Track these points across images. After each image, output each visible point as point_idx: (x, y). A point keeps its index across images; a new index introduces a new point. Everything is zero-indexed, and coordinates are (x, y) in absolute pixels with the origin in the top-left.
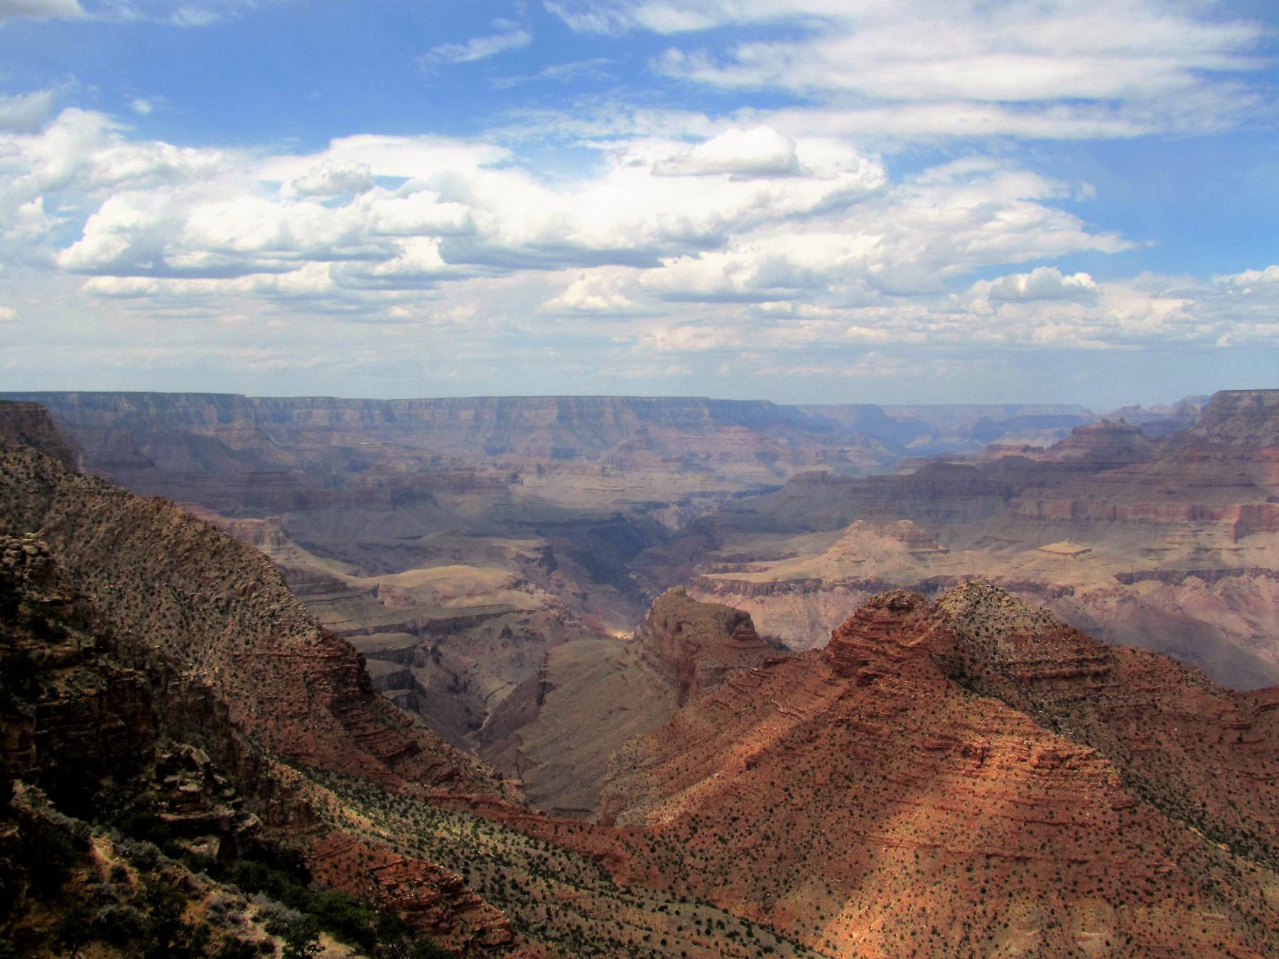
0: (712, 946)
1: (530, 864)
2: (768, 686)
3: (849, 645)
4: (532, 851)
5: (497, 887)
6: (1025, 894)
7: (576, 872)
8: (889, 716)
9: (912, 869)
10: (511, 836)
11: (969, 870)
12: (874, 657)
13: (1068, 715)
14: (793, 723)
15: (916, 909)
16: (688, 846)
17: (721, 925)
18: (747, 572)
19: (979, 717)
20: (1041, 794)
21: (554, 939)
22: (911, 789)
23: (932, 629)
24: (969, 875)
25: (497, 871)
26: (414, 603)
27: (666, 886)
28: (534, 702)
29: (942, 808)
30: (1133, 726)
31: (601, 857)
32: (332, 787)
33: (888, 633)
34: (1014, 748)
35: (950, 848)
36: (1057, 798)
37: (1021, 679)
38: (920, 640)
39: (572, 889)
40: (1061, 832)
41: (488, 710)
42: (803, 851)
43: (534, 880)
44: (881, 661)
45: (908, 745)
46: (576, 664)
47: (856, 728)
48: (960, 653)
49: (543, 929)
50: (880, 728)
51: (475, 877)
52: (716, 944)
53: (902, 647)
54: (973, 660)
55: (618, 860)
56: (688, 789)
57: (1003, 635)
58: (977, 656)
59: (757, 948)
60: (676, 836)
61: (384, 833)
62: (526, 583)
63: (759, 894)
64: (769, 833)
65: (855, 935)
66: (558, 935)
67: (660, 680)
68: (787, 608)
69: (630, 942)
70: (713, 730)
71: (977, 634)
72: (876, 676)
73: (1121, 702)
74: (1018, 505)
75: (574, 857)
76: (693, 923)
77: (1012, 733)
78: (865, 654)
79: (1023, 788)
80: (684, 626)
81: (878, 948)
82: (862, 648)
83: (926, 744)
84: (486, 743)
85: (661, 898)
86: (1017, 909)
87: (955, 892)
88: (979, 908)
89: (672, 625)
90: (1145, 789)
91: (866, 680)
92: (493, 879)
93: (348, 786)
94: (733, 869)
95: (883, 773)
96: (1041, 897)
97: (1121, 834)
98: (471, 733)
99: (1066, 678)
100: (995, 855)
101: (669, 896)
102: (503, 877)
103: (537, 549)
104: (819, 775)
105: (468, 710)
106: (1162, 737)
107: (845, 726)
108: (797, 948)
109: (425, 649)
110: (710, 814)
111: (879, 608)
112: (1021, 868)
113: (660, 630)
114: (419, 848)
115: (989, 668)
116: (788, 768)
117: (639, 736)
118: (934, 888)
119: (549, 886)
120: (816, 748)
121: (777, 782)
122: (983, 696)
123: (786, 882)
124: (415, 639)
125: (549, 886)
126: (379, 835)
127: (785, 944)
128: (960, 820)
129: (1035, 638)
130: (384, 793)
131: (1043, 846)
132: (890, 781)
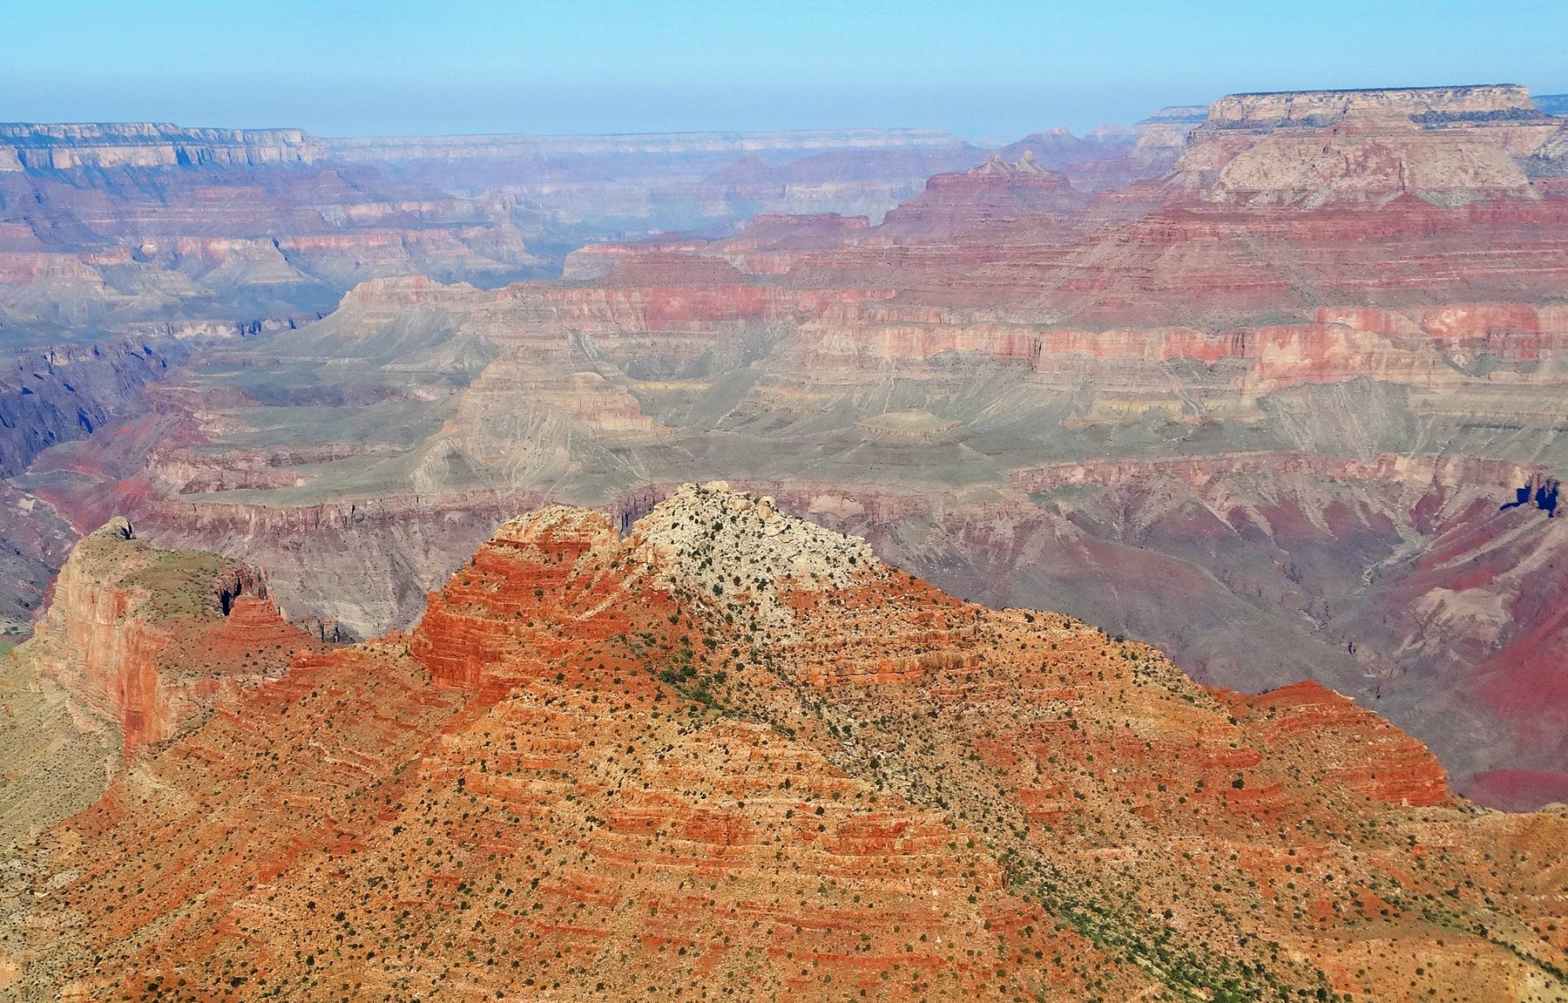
2: (302, 713)
13: (901, 747)
14: (356, 785)
20: (847, 906)
23: (626, 584)
30: (1033, 765)
38: (601, 608)
48: (683, 629)
57: (769, 592)
58: (718, 637)
70: (192, 806)
71: (718, 591)
73: (1006, 719)
78: (492, 641)
90: (1053, 888)
91: (499, 689)
97: (1001, 974)
104: (405, 887)
106: (1088, 785)
120: (397, 830)
122: (728, 715)
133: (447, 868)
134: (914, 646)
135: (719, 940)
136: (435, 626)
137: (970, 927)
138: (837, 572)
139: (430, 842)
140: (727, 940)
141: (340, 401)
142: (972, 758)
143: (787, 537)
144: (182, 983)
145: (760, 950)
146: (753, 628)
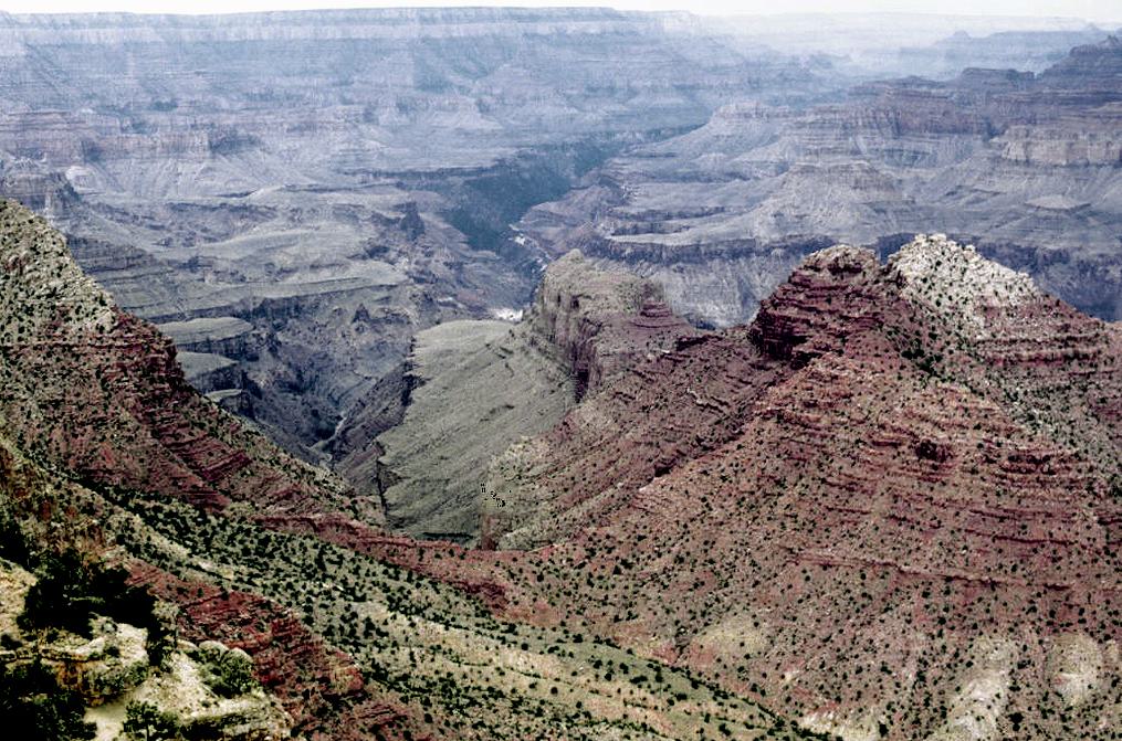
0: (614, 695)
1: (389, 598)
2: (683, 373)
3: (783, 317)
4: (390, 582)
5: (347, 628)
6: (993, 626)
7: (446, 607)
8: (830, 405)
9: (857, 592)
10: (365, 565)
11: (925, 595)
12: (812, 332)
14: (714, 418)
15: (863, 642)
16: (584, 571)
17: (624, 668)
18: (662, 232)
19: (939, 407)
21: (420, 689)
22: (856, 494)
24: (926, 602)
25: (347, 609)
26: (243, 279)
27: (556, 622)
28: (398, 400)
29: (893, 517)
31: (478, 589)
32: (139, 510)
33: (829, 301)
34: (980, 446)
35: (904, 568)
36: (1032, 509)
37: (991, 362)
39: (440, 627)
40: (1035, 551)
41: (342, 414)
42: (725, 576)
43: (394, 617)
44: (819, 337)
45: (853, 440)
46: (449, 352)
47: (789, 421)
48: (916, 326)
49: (405, 677)
50: (818, 420)
51: (321, 616)
52: (619, 691)
53: (847, 318)
54: (933, 336)
55: (497, 591)
56: (585, 503)
58: (938, 332)
59: (668, 695)
60: (569, 560)
61: (204, 566)
62: (386, 250)
63: (672, 630)
64: (683, 554)
65: (789, 676)
66: (422, 684)
67: (553, 369)
68: (712, 277)
69: (514, 691)
70: (616, 428)
71: (938, 304)
72: (814, 355)
74: (1001, 147)
75: (442, 587)
76: (590, 667)
77: (978, 427)
78: (800, 329)
79: (992, 498)
80: (581, 300)
81: (816, 691)
82: (795, 320)
83: (875, 438)
84: (339, 455)
85: (551, 637)
86: (983, 644)
87: (909, 622)
88: (938, 643)
89: (566, 301)
91: (804, 359)
92: (343, 618)
93: (158, 509)
94: (640, 600)
95: (822, 475)
96: (1011, 630)
98: (321, 443)
99: (1046, 361)
100: (958, 577)
101: (560, 634)
102: (355, 615)
103: (398, 207)
104: (744, 481)
105: (315, 413)
107: (775, 419)
108: (718, 693)
109: (258, 336)
110: (611, 533)
111: (818, 270)
112: (986, 594)
113: (551, 306)
114: (250, 582)
115: (952, 347)
116: (705, 473)
117: (526, 438)
118: (884, 616)
119: (413, 625)
120: (739, 447)
121: (692, 491)
123: (703, 614)
124: (247, 326)
125: (413, 625)
126: (198, 568)
127: (703, 689)
128: (915, 534)
129: (1011, 311)
130: (203, 515)
131: (1014, 569)
132: (832, 485)
133: (769, 470)
134: (1058, 344)
135: (935, 522)
136: (764, 318)
137: (1090, 522)
138: (1012, 295)
139: (759, 454)
140: (939, 522)
141: (710, 180)
142: (1093, 415)
143: (981, 272)
144: (608, 537)
145: (959, 530)
146: (960, 328)
